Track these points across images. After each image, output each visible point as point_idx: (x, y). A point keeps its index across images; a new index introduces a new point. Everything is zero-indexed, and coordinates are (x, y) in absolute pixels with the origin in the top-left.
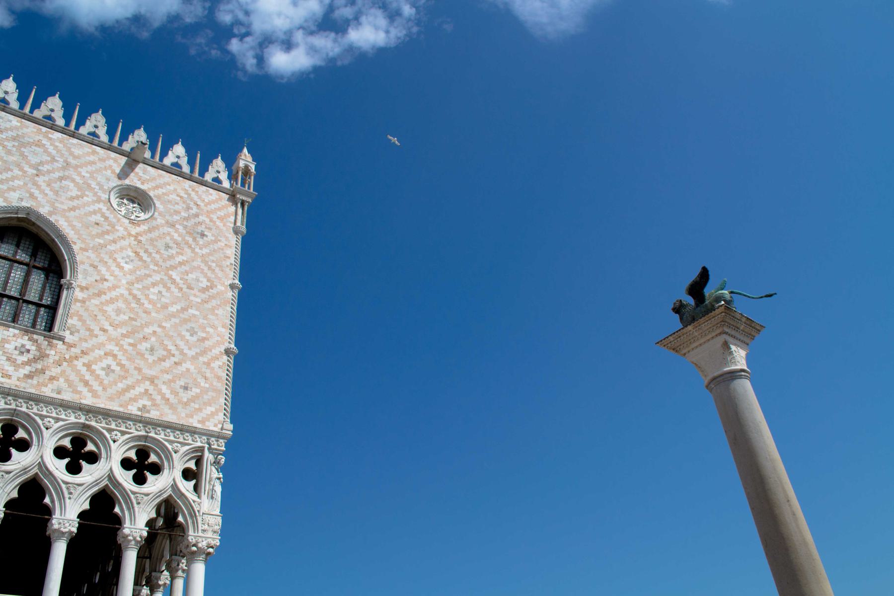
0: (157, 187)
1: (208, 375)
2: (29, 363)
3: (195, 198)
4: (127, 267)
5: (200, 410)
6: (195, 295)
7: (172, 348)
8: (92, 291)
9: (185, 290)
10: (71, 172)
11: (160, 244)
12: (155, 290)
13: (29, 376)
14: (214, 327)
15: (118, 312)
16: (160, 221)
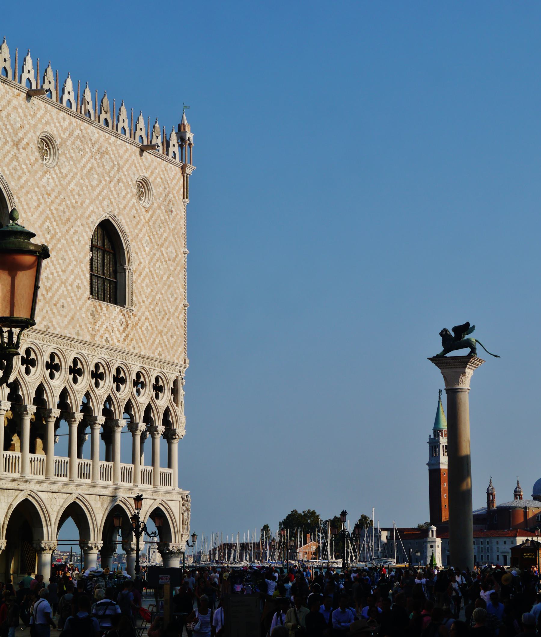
0: (152, 173)
1: (179, 326)
2: (123, 331)
3: (168, 179)
4: (147, 249)
5: (176, 351)
6: (172, 266)
7: (166, 308)
8: (138, 273)
9: (168, 262)
10: (121, 174)
11: (157, 226)
12: (157, 266)
13: (125, 340)
14: (179, 289)
15: (147, 286)
16: (156, 205)
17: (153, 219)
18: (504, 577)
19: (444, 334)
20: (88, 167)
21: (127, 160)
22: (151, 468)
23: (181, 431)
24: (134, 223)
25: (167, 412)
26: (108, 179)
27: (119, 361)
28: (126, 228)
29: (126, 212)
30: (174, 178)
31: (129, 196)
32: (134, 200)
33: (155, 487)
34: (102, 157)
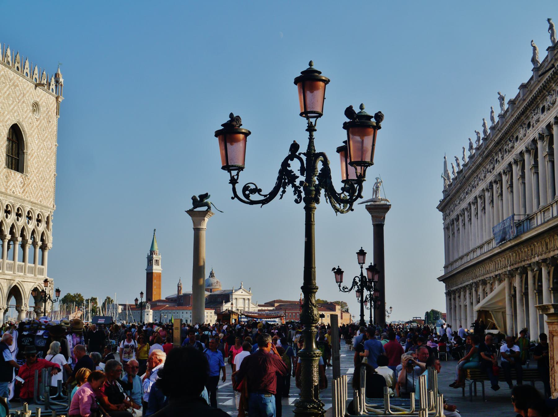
0: (41, 99)
4: (37, 142)
11: (42, 129)
15: (36, 163)
17: (40, 125)
18: (259, 325)
19: (194, 199)
20: (7, 93)
21: (28, 91)
22: (33, 265)
23: (50, 245)
24: (30, 127)
25: (43, 234)
26: (17, 101)
27: (19, 204)
28: (26, 129)
29: (26, 120)
30: (52, 103)
31: (28, 111)
32: (31, 114)
33: (35, 275)
34: (15, 88)
